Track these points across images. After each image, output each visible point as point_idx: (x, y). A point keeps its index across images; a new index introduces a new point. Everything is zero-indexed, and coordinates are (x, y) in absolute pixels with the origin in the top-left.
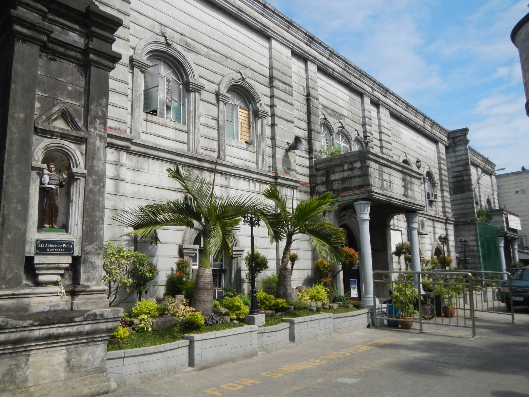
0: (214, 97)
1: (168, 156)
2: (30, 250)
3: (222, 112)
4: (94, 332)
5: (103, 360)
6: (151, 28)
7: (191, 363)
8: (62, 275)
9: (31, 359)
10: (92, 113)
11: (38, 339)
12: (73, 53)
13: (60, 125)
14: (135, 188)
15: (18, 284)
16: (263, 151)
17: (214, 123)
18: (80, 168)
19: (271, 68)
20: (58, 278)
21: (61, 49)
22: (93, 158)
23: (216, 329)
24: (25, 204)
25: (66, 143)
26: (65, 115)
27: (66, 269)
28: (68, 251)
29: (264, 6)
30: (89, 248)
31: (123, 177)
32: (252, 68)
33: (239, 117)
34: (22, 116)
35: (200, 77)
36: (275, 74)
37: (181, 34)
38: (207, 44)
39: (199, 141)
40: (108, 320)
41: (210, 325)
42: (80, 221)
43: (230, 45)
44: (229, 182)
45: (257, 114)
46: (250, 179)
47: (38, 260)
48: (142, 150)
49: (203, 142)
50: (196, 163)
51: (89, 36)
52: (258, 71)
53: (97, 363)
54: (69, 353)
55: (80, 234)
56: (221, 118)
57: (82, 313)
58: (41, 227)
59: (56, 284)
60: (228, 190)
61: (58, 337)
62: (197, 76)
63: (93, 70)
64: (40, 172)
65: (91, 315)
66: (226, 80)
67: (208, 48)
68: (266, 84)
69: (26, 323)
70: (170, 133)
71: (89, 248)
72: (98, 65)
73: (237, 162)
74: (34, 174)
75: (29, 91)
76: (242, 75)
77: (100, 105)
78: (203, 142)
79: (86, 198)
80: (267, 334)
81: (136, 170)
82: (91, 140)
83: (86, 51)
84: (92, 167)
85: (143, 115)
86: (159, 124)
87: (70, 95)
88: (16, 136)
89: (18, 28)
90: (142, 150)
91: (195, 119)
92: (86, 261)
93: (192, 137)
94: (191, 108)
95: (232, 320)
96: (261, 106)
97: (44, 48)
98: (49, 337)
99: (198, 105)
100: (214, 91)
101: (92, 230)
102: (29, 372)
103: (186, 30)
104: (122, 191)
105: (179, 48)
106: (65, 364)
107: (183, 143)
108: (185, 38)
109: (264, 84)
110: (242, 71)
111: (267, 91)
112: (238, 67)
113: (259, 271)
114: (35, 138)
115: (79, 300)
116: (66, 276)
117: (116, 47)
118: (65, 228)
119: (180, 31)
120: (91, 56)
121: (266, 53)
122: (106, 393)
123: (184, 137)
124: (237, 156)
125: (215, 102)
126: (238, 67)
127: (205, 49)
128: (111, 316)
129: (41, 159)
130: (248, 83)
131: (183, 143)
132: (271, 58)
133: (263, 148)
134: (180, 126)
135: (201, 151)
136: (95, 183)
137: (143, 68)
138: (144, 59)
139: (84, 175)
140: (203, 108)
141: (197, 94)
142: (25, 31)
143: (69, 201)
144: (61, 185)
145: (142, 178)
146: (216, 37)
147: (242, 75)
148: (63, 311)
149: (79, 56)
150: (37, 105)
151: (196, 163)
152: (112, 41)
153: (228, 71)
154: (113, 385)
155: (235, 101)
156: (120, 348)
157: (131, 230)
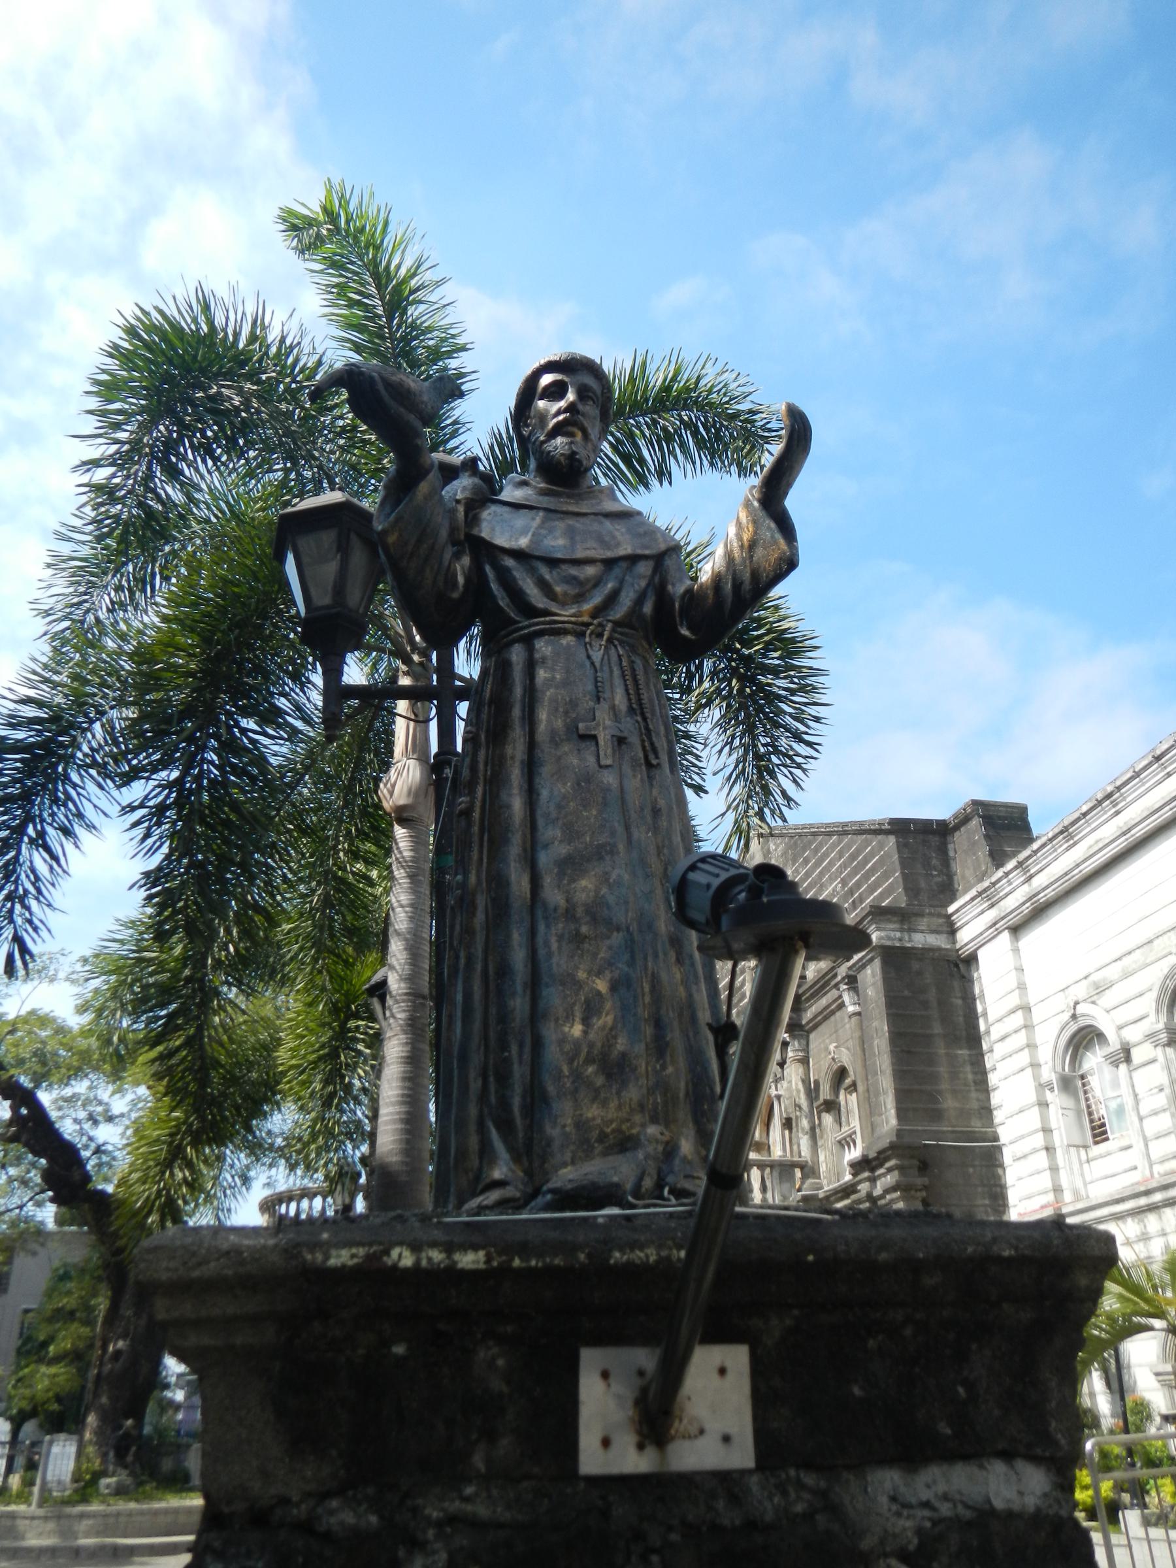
37: (1086, 978)
67: (1120, 959)
108: (1091, 979)
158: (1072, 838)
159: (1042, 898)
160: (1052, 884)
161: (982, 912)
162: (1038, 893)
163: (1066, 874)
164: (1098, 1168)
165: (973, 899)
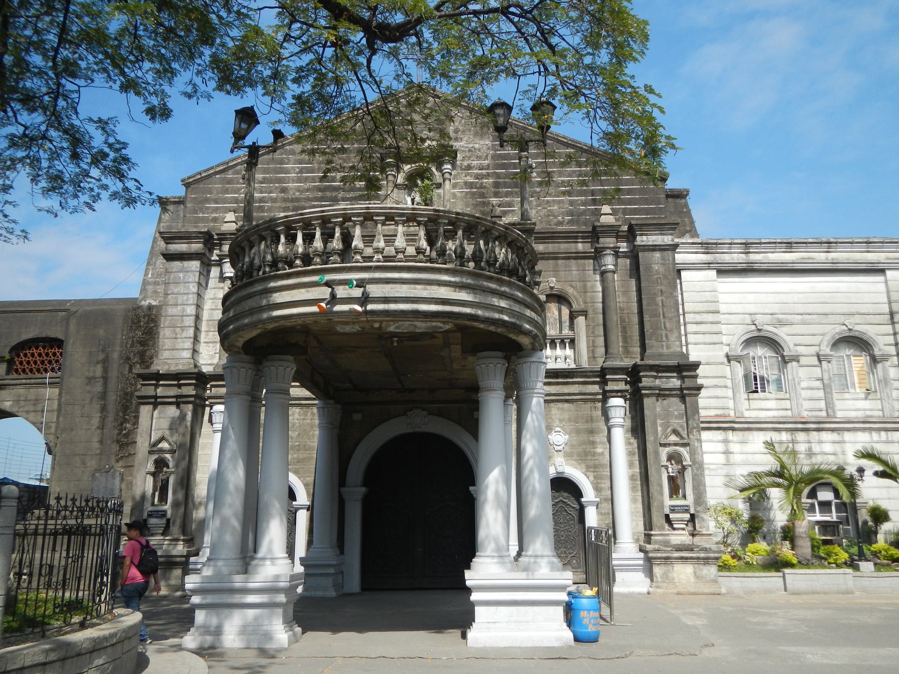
0: (816, 358)
1: (770, 426)
2: (667, 511)
3: (826, 371)
4: (707, 558)
5: (715, 576)
6: (742, 322)
7: (786, 590)
8: (687, 525)
9: (675, 568)
10: (690, 426)
11: (676, 558)
12: (674, 392)
13: (673, 438)
14: (743, 457)
15: (663, 529)
16: (888, 397)
17: (818, 384)
18: (687, 461)
19: (890, 303)
20: (684, 526)
21: (668, 392)
22: (695, 454)
23: (809, 568)
24: (661, 486)
25: (677, 448)
26: (675, 432)
27: (688, 521)
28: (687, 511)
29: (866, 243)
30: (699, 509)
31: (731, 451)
32: (863, 311)
33: (853, 365)
34: (652, 438)
35: (796, 345)
36: (895, 307)
38: (801, 311)
39: (802, 405)
40: (714, 552)
41: (804, 564)
42: (692, 493)
43: (828, 301)
44: (842, 437)
45: (874, 360)
46: (870, 430)
47: (672, 516)
48: (746, 426)
49: (807, 405)
50: (800, 426)
51: (682, 378)
52: (871, 311)
53: (712, 577)
54: (695, 568)
55: (693, 501)
56: (826, 377)
57: (698, 546)
58: (671, 497)
59: (683, 529)
60: (842, 445)
61: (687, 558)
62: (792, 346)
63: (687, 399)
64: (666, 467)
65: (703, 548)
66: (828, 338)
67: (802, 314)
68: (886, 322)
69: (669, 549)
70: (771, 404)
71: (699, 509)
72: (689, 395)
73: (852, 415)
74: (663, 469)
75: (654, 423)
76: (847, 326)
77: (694, 420)
78: (807, 405)
79: (694, 479)
80: (866, 579)
81: (743, 442)
82: (691, 443)
83: (681, 389)
84: (695, 459)
85: (745, 396)
86: (760, 399)
87: (677, 417)
88: (651, 450)
89: (643, 392)
90: (746, 426)
91: (795, 386)
92: (698, 517)
93: (794, 403)
94: (790, 378)
95: (829, 563)
96: (880, 350)
97: (658, 396)
98: (682, 558)
99: (797, 372)
100: (814, 353)
101: (699, 498)
102: (675, 575)
103: (775, 309)
104: (732, 461)
105: (770, 328)
106: (693, 574)
107: (787, 410)
109: (882, 323)
110: (846, 322)
111: (889, 329)
112: (842, 319)
113: (881, 523)
114: (661, 448)
115: (697, 539)
116: (689, 525)
117: (700, 381)
118: (684, 497)
119: (770, 312)
120: (685, 392)
121: (882, 287)
122: (719, 594)
123: (787, 404)
124: (853, 408)
125: (817, 363)
126: (842, 319)
127: (800, 317)
128: (716, 549)
129: (666, 460)
130: (857, 331)
131: (787, 410)
132: (888, 292)
133: (887, 394)
134: (782, 395)
135: (805, 414)
136: (697, 469)
137: (738, 359)
138: (739, 351)
139: (690, 466)
140: (803, 373)
141: (794, 364)
142: (647, 392)
143: (684, 481)
144: (679, 472)
145: (749, 448)
146: (810, 301)
147: (847, 326)
148: (689, 545)
149: (678, 392)
150: (659, 429)
151: (800, 426)
152: (696, 377)
153: (829, 327)
154: (724, 591)
155: (846, 351)
156: (730, 571)
157: (738, 492)
158: (791, 248)
159: (756, 266)
160: (769, 263)
161: (697, 253)
162: (756, 263)
163: (782, 263)
164: (755, 404)
165: (693, 243)
